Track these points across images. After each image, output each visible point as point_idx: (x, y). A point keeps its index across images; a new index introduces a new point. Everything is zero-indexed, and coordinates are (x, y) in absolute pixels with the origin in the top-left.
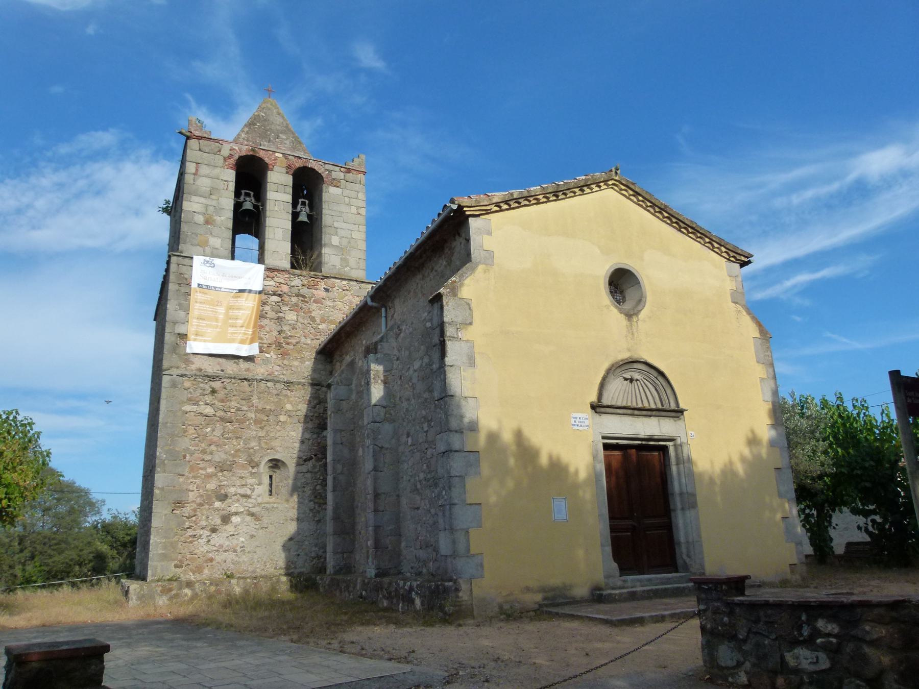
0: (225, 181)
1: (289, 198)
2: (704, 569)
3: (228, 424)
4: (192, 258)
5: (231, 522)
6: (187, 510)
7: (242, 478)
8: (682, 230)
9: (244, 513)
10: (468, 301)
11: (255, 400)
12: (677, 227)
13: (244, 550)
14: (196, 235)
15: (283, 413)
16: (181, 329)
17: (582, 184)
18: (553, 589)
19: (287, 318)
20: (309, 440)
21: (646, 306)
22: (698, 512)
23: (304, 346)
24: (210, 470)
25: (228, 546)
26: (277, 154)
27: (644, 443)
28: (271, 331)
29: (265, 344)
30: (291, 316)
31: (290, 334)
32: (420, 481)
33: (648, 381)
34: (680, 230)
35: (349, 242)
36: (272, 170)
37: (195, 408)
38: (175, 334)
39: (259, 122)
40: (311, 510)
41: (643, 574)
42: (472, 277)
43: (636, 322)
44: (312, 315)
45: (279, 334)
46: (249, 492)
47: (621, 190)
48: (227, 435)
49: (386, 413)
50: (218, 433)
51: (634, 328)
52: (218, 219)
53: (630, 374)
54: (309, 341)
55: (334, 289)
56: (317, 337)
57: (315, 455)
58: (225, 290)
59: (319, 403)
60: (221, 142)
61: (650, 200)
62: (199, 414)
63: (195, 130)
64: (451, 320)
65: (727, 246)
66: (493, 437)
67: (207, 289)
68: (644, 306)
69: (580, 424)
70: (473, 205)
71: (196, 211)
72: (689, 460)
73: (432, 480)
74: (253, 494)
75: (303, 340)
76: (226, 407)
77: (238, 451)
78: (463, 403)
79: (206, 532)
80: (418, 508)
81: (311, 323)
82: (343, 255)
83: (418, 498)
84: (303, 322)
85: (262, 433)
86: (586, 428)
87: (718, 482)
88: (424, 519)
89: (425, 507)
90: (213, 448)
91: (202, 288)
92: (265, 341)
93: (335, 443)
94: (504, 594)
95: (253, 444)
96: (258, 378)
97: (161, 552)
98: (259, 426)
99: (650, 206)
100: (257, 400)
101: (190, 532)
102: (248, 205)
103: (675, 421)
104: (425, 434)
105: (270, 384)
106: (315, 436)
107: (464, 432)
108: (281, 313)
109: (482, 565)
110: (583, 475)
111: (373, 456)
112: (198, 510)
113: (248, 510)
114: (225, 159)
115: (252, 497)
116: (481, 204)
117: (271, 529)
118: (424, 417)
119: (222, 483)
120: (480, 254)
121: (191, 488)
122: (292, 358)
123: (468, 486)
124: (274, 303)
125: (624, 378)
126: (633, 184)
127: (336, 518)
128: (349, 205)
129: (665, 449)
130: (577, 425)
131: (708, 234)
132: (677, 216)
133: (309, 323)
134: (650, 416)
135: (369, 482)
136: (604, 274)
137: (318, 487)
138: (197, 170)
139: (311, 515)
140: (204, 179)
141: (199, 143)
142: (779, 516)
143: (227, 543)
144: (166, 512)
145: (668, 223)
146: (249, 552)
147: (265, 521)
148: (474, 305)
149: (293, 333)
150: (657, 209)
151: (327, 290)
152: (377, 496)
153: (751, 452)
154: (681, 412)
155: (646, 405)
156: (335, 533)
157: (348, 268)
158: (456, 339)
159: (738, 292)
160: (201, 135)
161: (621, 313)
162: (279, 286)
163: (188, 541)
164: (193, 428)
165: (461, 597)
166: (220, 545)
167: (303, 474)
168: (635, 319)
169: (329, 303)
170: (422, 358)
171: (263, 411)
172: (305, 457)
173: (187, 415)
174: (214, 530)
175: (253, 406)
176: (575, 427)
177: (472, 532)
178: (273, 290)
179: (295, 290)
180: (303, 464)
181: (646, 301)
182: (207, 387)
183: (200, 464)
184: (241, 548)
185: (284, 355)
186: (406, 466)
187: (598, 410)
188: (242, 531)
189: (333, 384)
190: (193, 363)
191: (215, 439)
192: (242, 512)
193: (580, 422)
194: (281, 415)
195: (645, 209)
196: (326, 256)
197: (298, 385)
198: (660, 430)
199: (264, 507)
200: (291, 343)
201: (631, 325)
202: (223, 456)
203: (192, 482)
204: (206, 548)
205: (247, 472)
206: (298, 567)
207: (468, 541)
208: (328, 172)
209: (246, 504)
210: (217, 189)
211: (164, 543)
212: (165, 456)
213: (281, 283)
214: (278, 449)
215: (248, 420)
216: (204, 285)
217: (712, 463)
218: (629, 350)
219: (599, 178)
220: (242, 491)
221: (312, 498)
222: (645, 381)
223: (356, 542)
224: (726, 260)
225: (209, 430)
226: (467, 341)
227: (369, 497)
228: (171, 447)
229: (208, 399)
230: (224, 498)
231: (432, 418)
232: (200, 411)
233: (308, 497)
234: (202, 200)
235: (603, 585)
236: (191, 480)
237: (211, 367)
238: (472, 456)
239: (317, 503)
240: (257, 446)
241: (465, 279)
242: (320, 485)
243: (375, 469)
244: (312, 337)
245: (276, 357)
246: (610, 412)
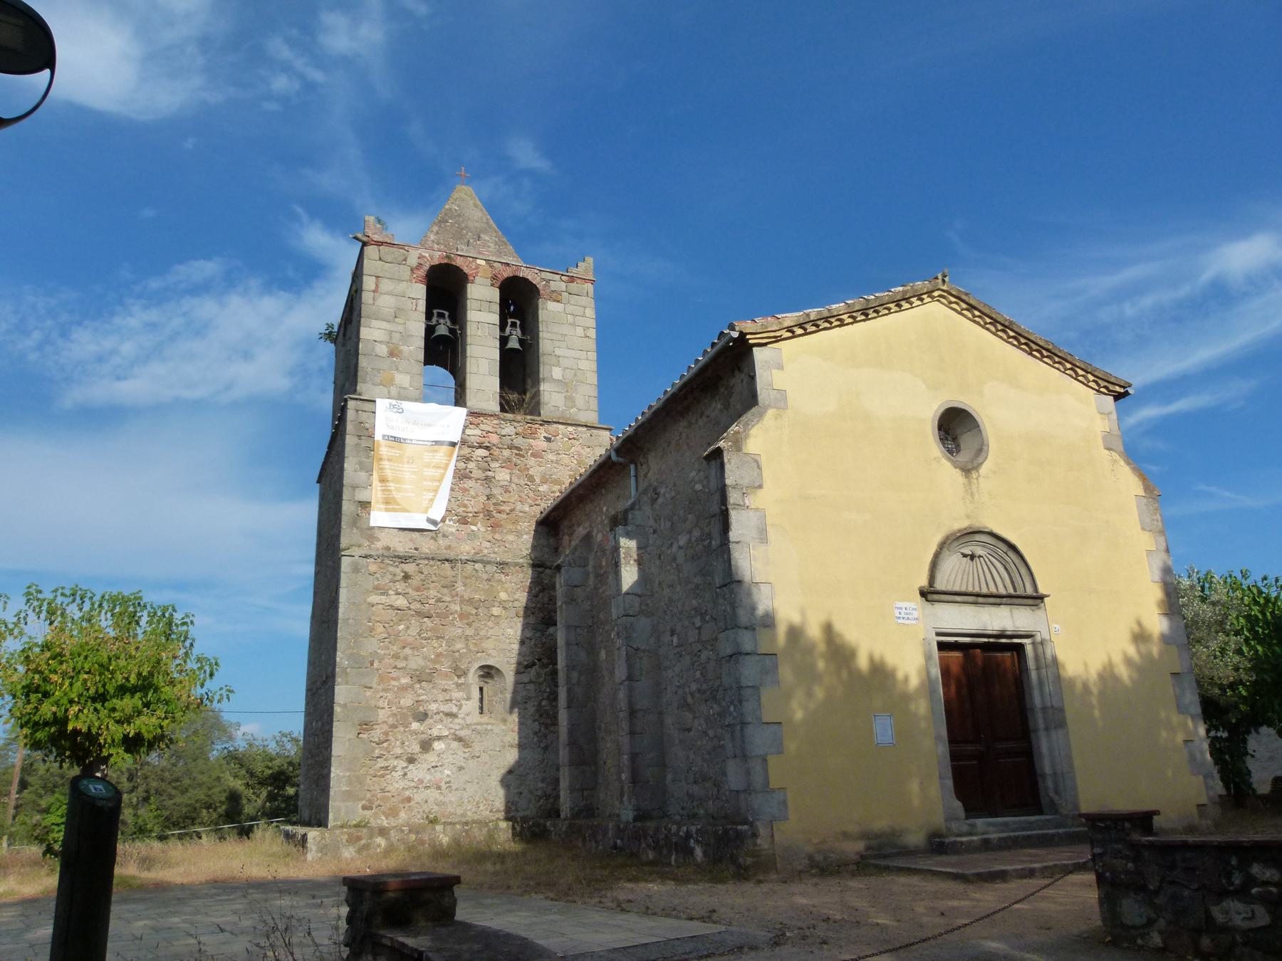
0: (413, 299)
1: (496, 318)
3: (426, 619)
4: (375, 401)
5: (433, 749)
6: (377, 734)
7: (445, 690)
8: (1034, 353)
9: (450, 737)
10: (756, 457)
11: (460, 588)
12: (1027, 349)
13: (451, 787)
14: (379, 370)
16: (362, 496)
17: (899, 298)
18: (877, 836)
19: (497, 478)
20: (531, 639)
21: (989, 457)
22: (1068, 732)
23: (521, 514)
24: (405, 681)
25: (429, 781)
26: (479, 262)
27: (991, 640)
28: (477, 495)
29: (470, 512)
30: (503, 475)
31: (502, 499)
32: (692, 694)
33: (993, 557)
34: (1031, 354)
35: (575, 375)
36: (473, 282)
37: (383, 599)
38: (355, 501)
39: (450, 218)
40: (536, 733)
41: (997, 816)
42: (759, 425)
43: (977, 479)
44: (530, 473)
45: (488, 499)
46: (455, 710)
47: (951, 303)
49: (641, 604)
50: (414, 631)
51: (974, 487)
52: (405, 348)
53: (970, 548)
54: (527, 509)
55: (557, 437)
56: (537, 503)
57: (539, 660)
58: (418, 442)
59: (543, 590)
60: (406, 248)
62: (389, 607)
63: (374, 234)
64: (734, 483)
65: (1096, 373)
66: (795, 633)
67: (395, 441)
68: (986, 458)
69: (906, 616)
70: (758, 331)
71: (377, 339)
72: (1055, 659)
73: (708, 692)
75: (519, 506)
76: (422, 597)
77: (439, 655)
78: (754, 591)
79: (402, 762)
80: (689, 730)
81: (529, 483)
82: (567, 391)
83: (689, 716)
84: (518, 482)
85: (470, 632)
86: (914, 622)
87: (1095, 691)
88: (699, 743)
89: (700, 728)
90: (408, 651)
91: (388, 440)
92: (470, 509)
93: (568, 644)
94: (815, 841)
95: (459, 646)
96: (463, 558)
97: (345, 788)
99: (990, 323)
100: (463, 588)
101: (381, 763)
102: (442, 330)
103: (1033, 610)
104: (697, 631)
105: (478, 566)
106: (538, 634)
107: (757, 628)
108: (490, 471)
109: (784, 803)
110: (914, 682)
111: (627, 661)
112: (390, 733)
114: (412, 270)
115: (459, 716)
117: (485, 758)
118: (695, 609)
119: (421, 698)
121: (381, 704)
122: (505, 531)
123: (763, 700)
124: (480, 459)
125: (962, 554)
126: (967, 294)
127: (572, 743)
128: (574, 325)
129: (1020, 647)
130: (903, 618)
131: (1069, 358)
132: (1026, 335)
133: (526, 484)
134: (1000, 604)
135: (622, 695)
136: (932, 415)
137: (544, 703)
138: (377, 286)
139: (535, 739)
140: (386, 297)
141: (379, 251)
142: (1180, 738)
143: (428, 777)
144: (350, 736)
145: (1014, 345)
146: (456, 789)
147: (477, 748)
148: (763, 461)
149: (505, 497)
150: (1000, 327)
151: (548, 440)
152: (632, 713)
153: (1139, 651)
154: (1041, 598)
155: (993, 590)
156: (572, 763)
157: (575, 409)
158: (742, 508)
159: (1112, 435)
160: (381, 240)
161: (956, 467)
162: (486, 435)
163: (379, 774)
164: (381, 625)
165: (760, 845)
167: (523, 685)
168: (974, 475)
169: (551, 457)
170: (690, 532)
171: (470, 601)
172: (525, 663)
173: (374, 609)
174: (411, 760)
175: (457, 595)
176: (900, 621)
177: (772, 761)
178: (478, 441)
179: (507, 440)
180: (524, 672)
181: (988, 450)
182: (398, 571)
183: (391, 673)
185: (495, 526)
186: (670, 673)
187: (930, 597)
188: (446, 761)
189: (564, 565)
190: (378, 540)
191: (410, 639)
192: (447, 736)
193: (907, 614)
194: (494, 606)
195: (983, 327)
196: (546, 393)
197: (514, 567)
198: (1014, 623)
199: (475, 729)
200: (504, 511)
201: (970, 483)
202: (421, 662)
203: (381, 697)
204: (401, 784)
205: (451, 682)
206: (520, 809)
207: (766, 771)
208: (544, 282)
209: (451, 726)
210: (403, 310)
211: (349, 776)
212: (347, 662)
213: (489, 432)
214: (491, 652)
215: (451, 614)
216: (391, 437)
217: (1086, 665)
218: (968, 517)
219: (921, 289)
220: (445, 708)
221: (536, 718)
222: (990, 557)
223: (600, 776)
224: (1095, 392)
225: (402, 627)
226: (757, 509)
227: (622, 715)
228: (355, 651)
229: (400, 586)
230: (423, 717)
231: (706, 611)
232: (390, 603)
233: (532, 715)
234: (385, 325)
236: (381, 694)
237: (402, 545)
238: (767, 661)
239: (543, 723)
240: (463, 648)
241: (751, 428)
242: (546, 699)
243: (630, 678)
244: (531, 502)
245: (484, 530)
246: (945, 600)
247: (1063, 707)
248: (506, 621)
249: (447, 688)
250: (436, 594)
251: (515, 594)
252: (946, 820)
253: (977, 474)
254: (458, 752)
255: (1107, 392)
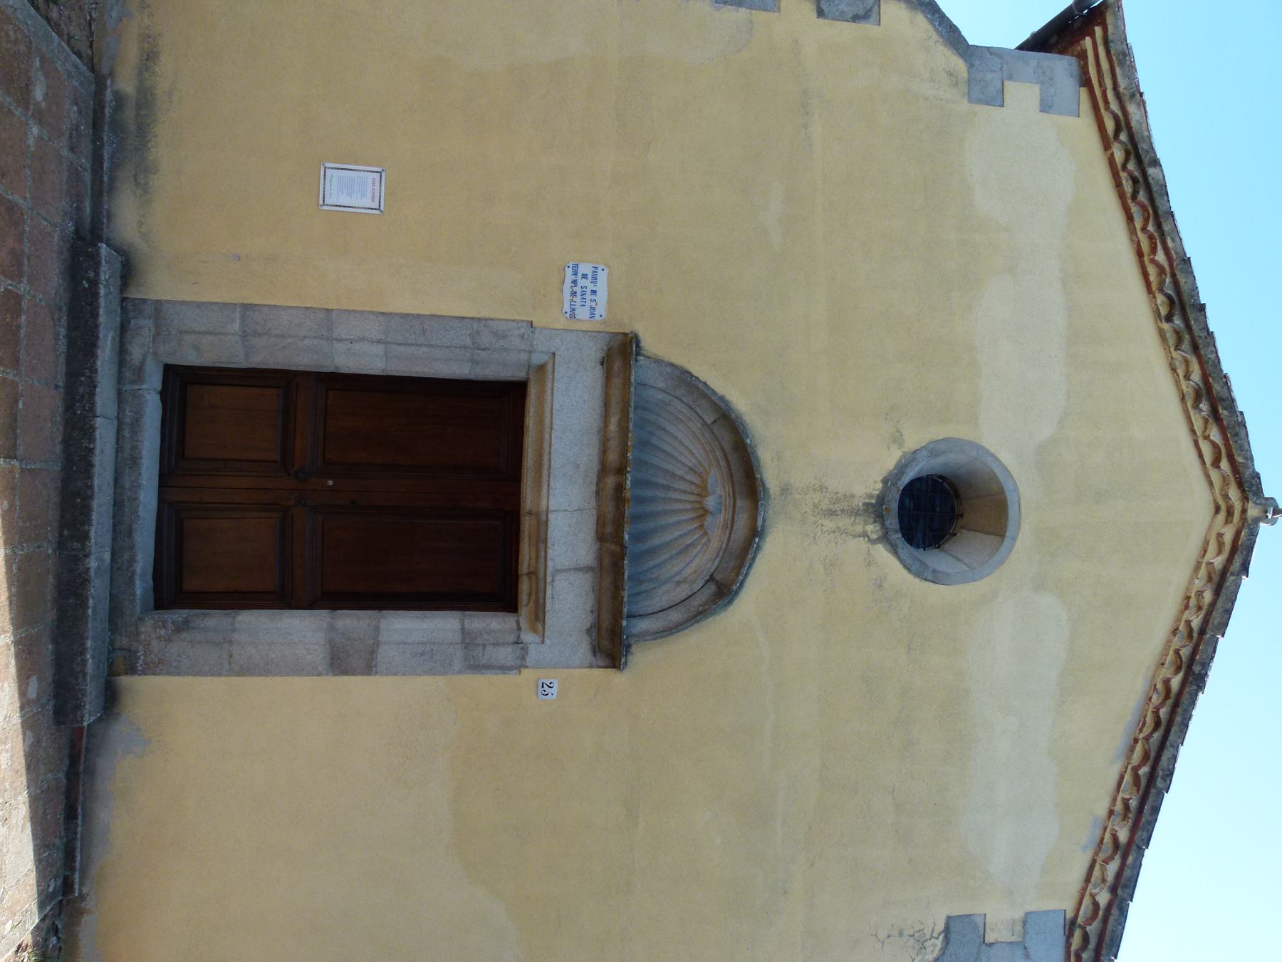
2: (144, 673)
10: (874, 15)
21: (910, 577)
22: (320, 674)
42: (935, 36)
43: (865, 535)
51: (844, 522)
61: (1210, 626)
68: (909, 570)
69: (578, 290)
86: (567, 308)
103: (589, 631)
116: (1118, 70)
120: (992, 71)
130: (575, 282)
132: (1178, 719)
136: (985, 444)
161: (885, 481)
168: (873, 529)
176: (569, 271)
181: (926, 580)
193: (584, 293)
198: (563, 571)
201: (855, 513)
235: (133, 294)
241: (927, 17)
247: (377, 673)
252: (159, 302)
253: (874, 536)
255: (1073, 948)
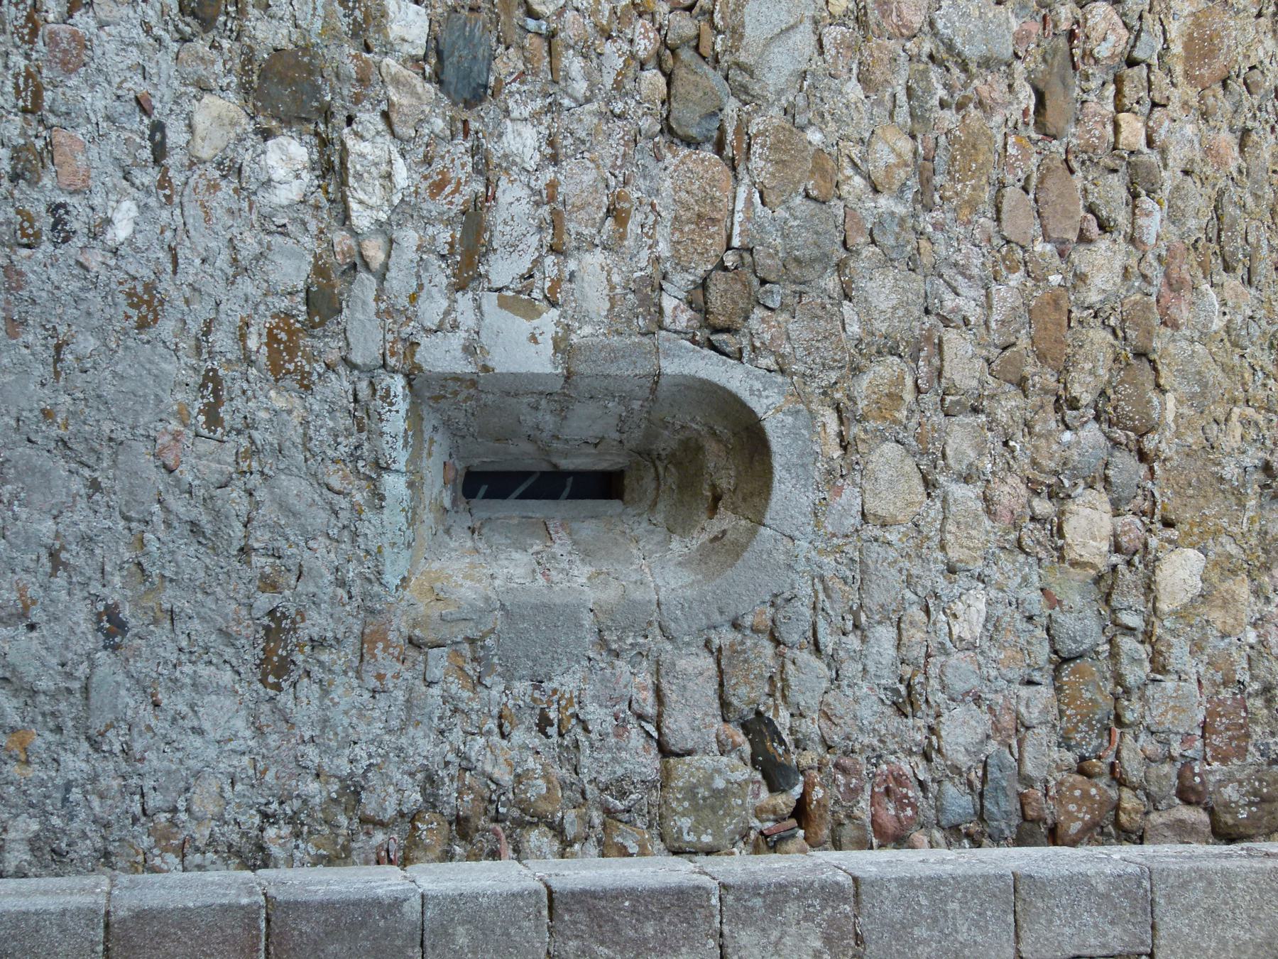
3: (1027, 98)
5: (266, 134)
7: (616, 213)
9: (341, 239)
15: (1131, 525)
40: (352, 792)
48: (941, 93)
74: (489, 301)
76: (1158, 76)
77: (822, 163)
98: (1023, 342)
100: (1218, 324)
113: (357, 264)
115: (464, 301)
119: (574, 64)
166: (82, 43)
167: (650, 710)
172: (783, 719)
175: (1175, 285)
180: (725, 705)
184: (54, 208)
188: (193, 211)
192: (345, 218)
194: (1117, 513)
205: (663, 249)
209: (409, 237)
221: (448, 791)
240: (866, 323)
248: (1033, 597)
249: (633, 227)
250: (1177, 156)
251: (1197, 647)
254: (245, 286)
